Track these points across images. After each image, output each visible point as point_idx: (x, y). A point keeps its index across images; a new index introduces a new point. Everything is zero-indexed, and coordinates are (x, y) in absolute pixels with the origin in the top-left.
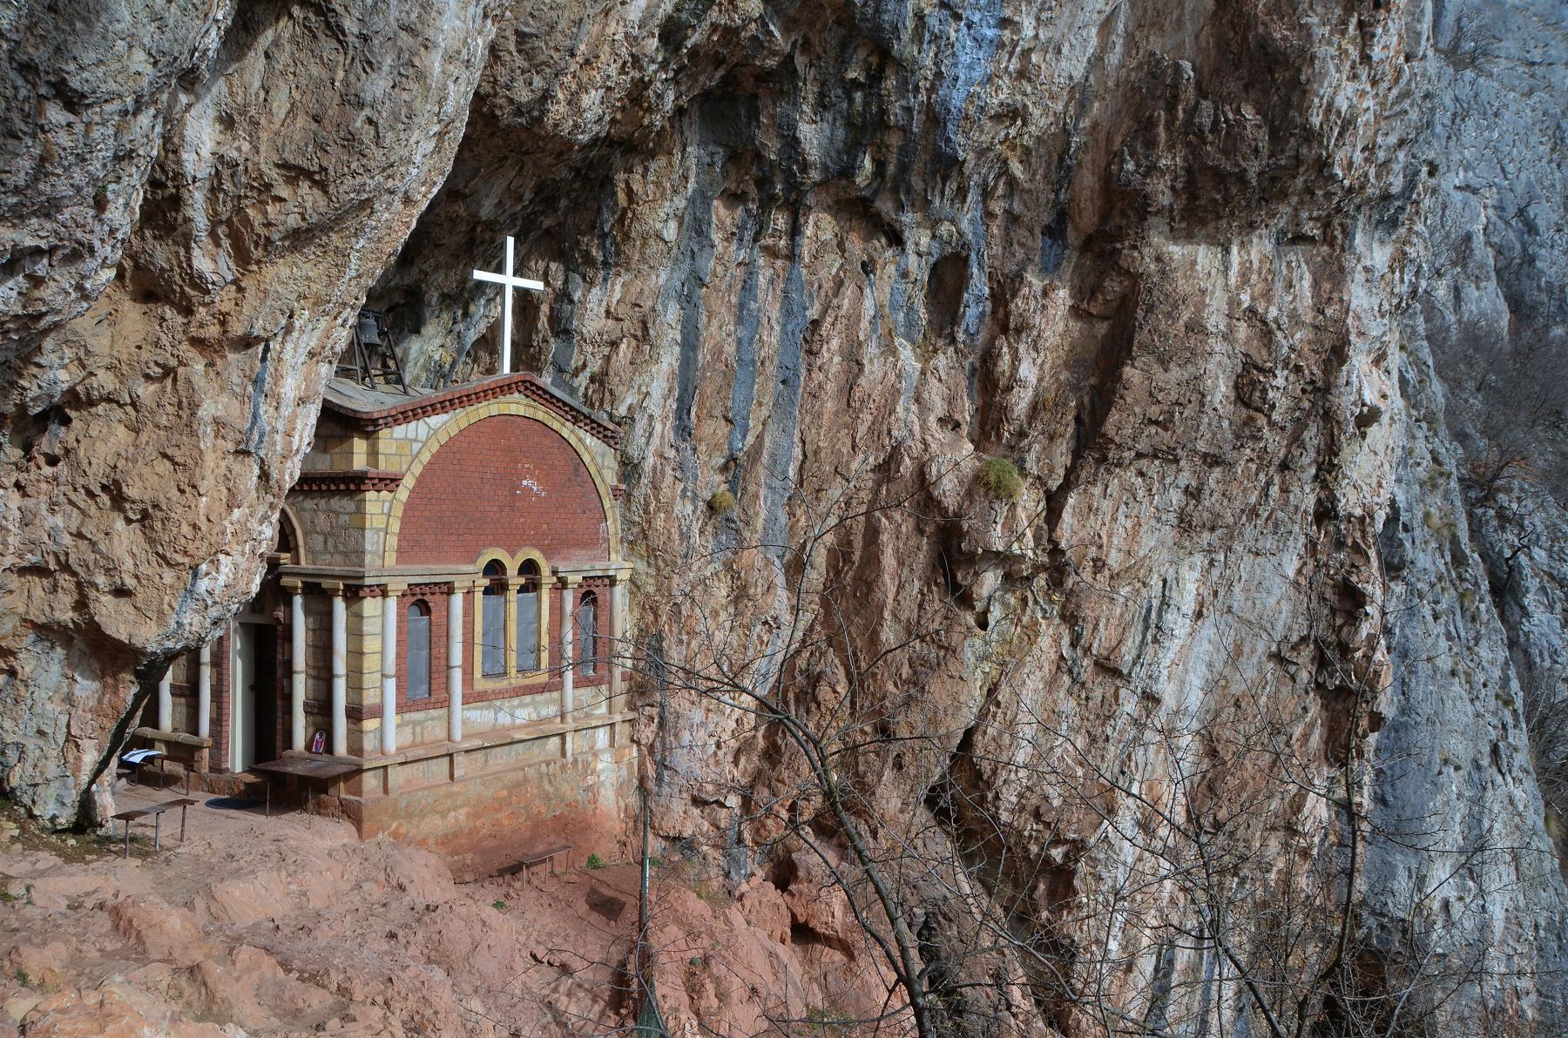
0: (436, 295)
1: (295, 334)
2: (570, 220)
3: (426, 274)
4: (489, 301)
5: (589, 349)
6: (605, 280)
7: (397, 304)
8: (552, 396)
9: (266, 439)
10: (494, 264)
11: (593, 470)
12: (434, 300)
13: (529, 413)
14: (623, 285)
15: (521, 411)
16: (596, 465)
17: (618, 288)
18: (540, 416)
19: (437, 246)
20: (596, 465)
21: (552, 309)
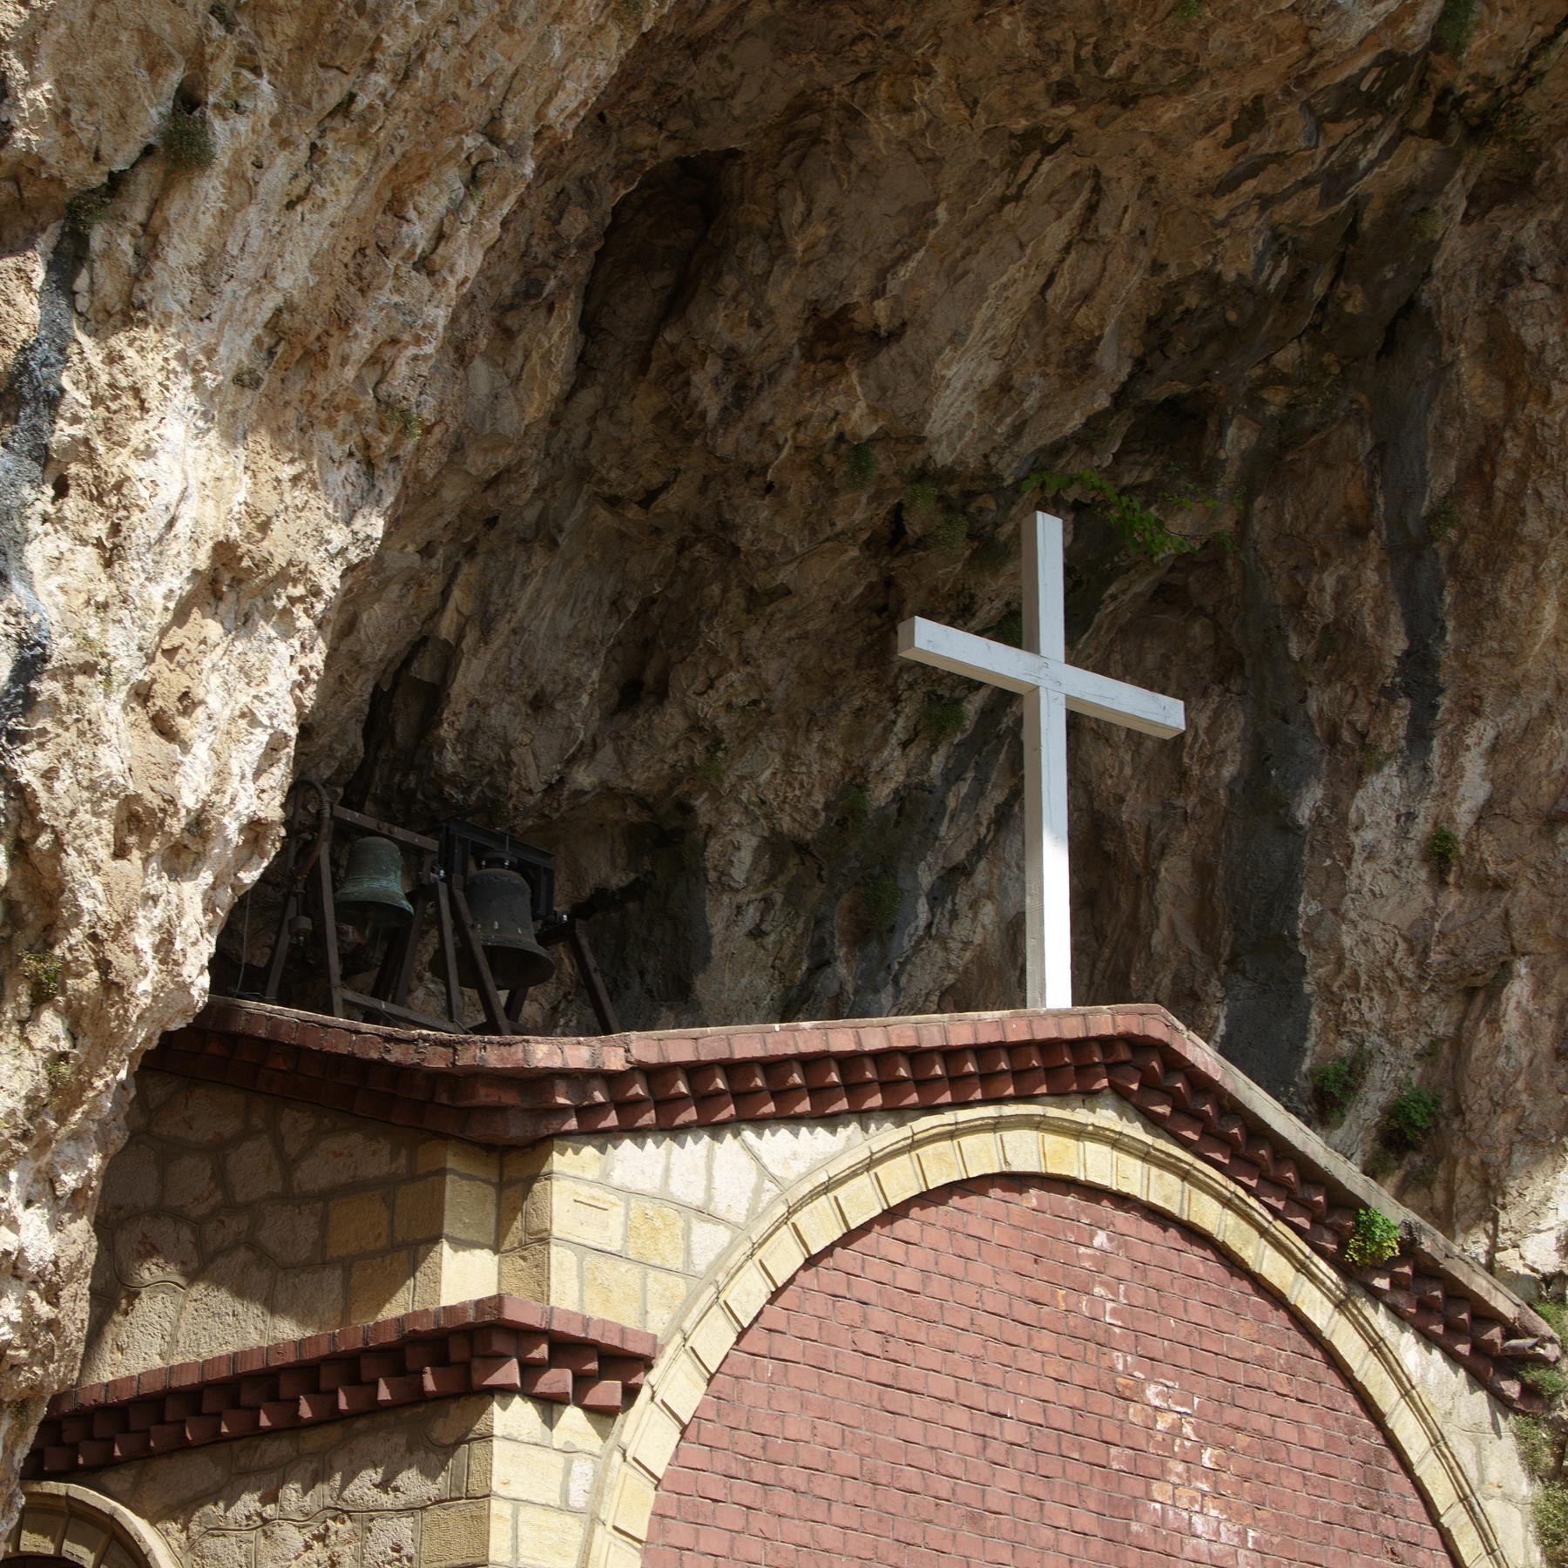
0: (748, 843)
1: (211, 189)
2: (1260, 526)
3: (716, 743)
4: (956, 874)
5: (1373, 1011)
6: (1419, 736)
7: (601, 893)
8: (1258, 1130)
9: (47, 687)
10: (972, 706)
11: (1442, 1492)
12: (745, 857)
13: (1163, 1190)
14: (1494, 751)
15: (1131, 1176)
16: (1454, 1470)
17: (1473, 765)
18: (1208, 1214)
19: (757, 600)
20: (1454, 1470)
21: (1203, 871)
